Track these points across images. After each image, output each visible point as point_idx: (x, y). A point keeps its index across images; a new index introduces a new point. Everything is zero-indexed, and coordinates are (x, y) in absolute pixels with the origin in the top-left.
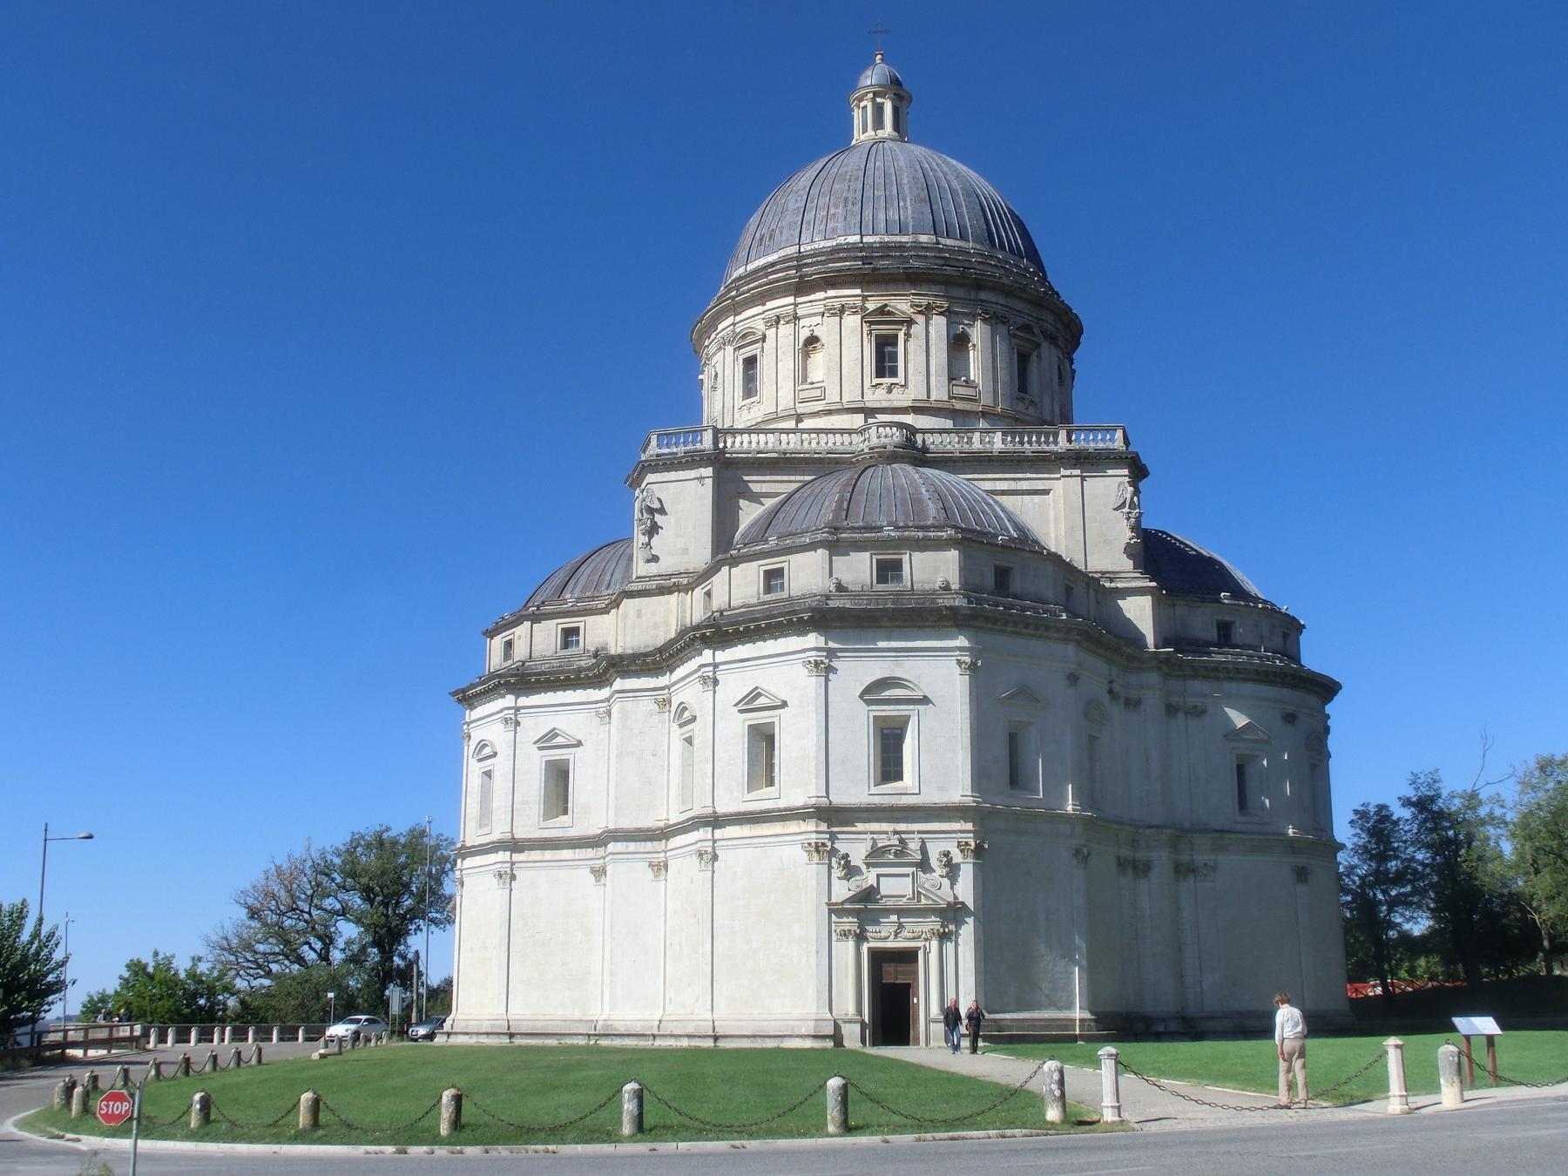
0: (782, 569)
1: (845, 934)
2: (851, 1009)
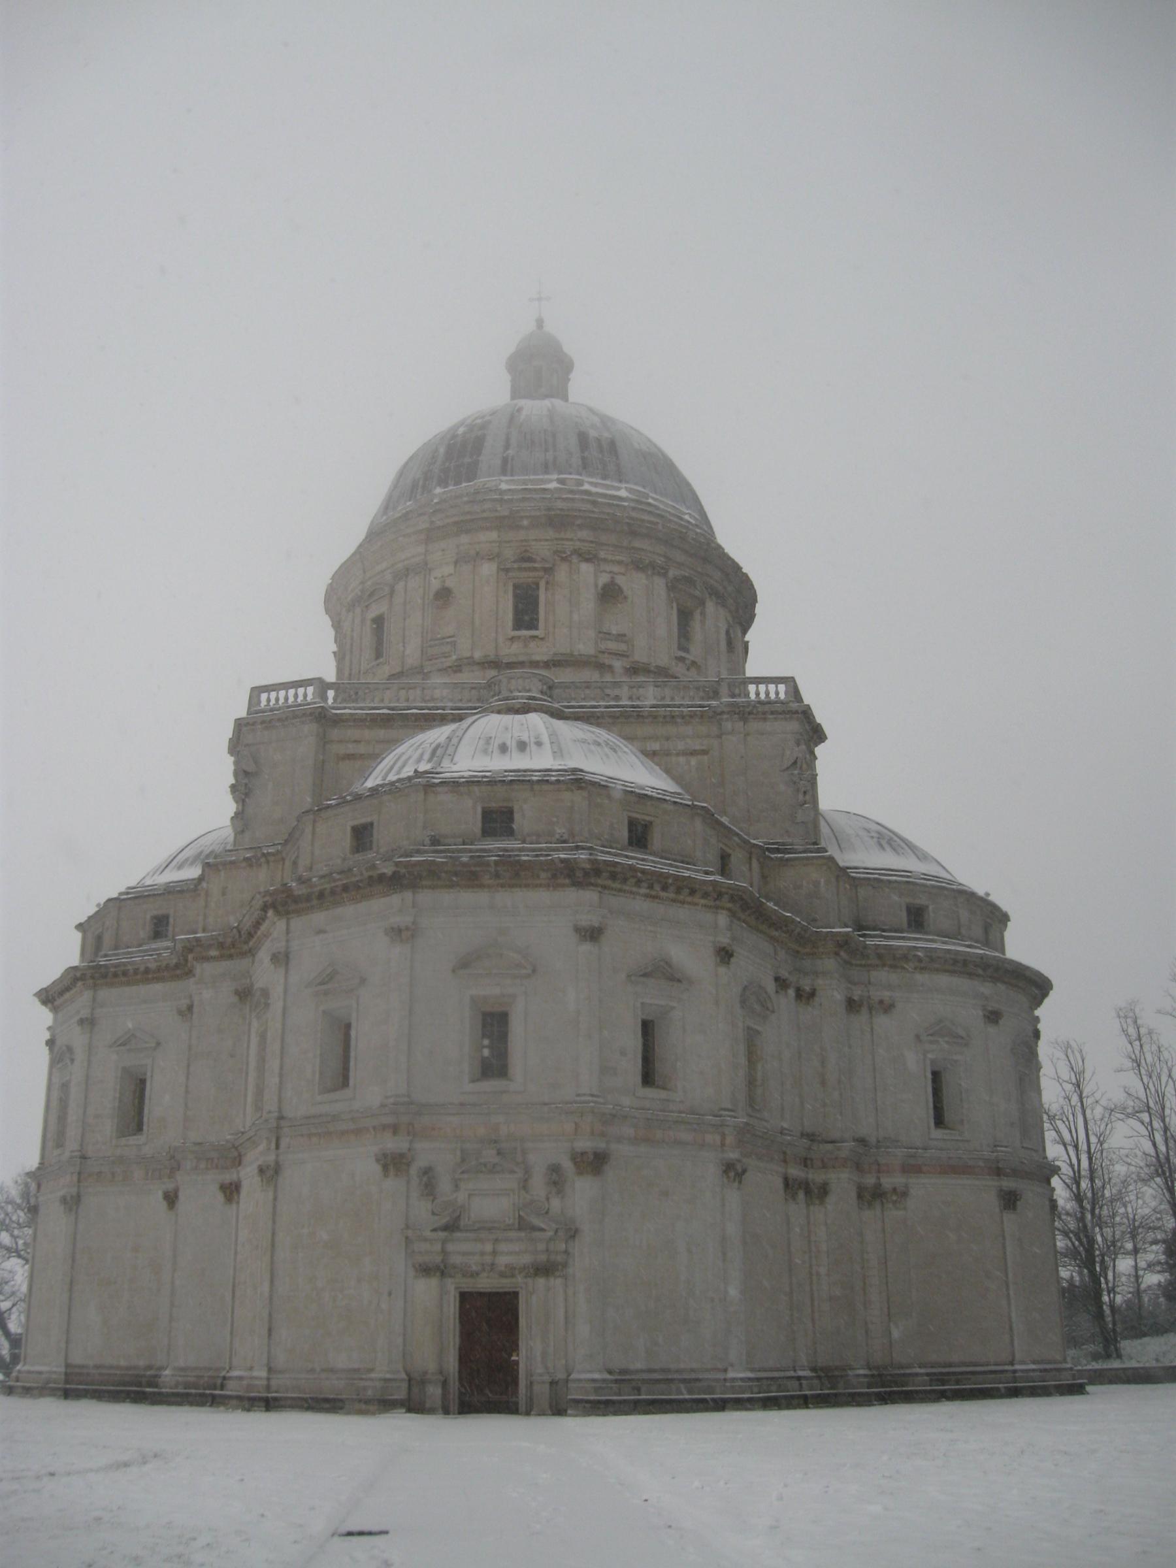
0: (372, 824)
1: (426, 1270)
2: (432, 1367)
